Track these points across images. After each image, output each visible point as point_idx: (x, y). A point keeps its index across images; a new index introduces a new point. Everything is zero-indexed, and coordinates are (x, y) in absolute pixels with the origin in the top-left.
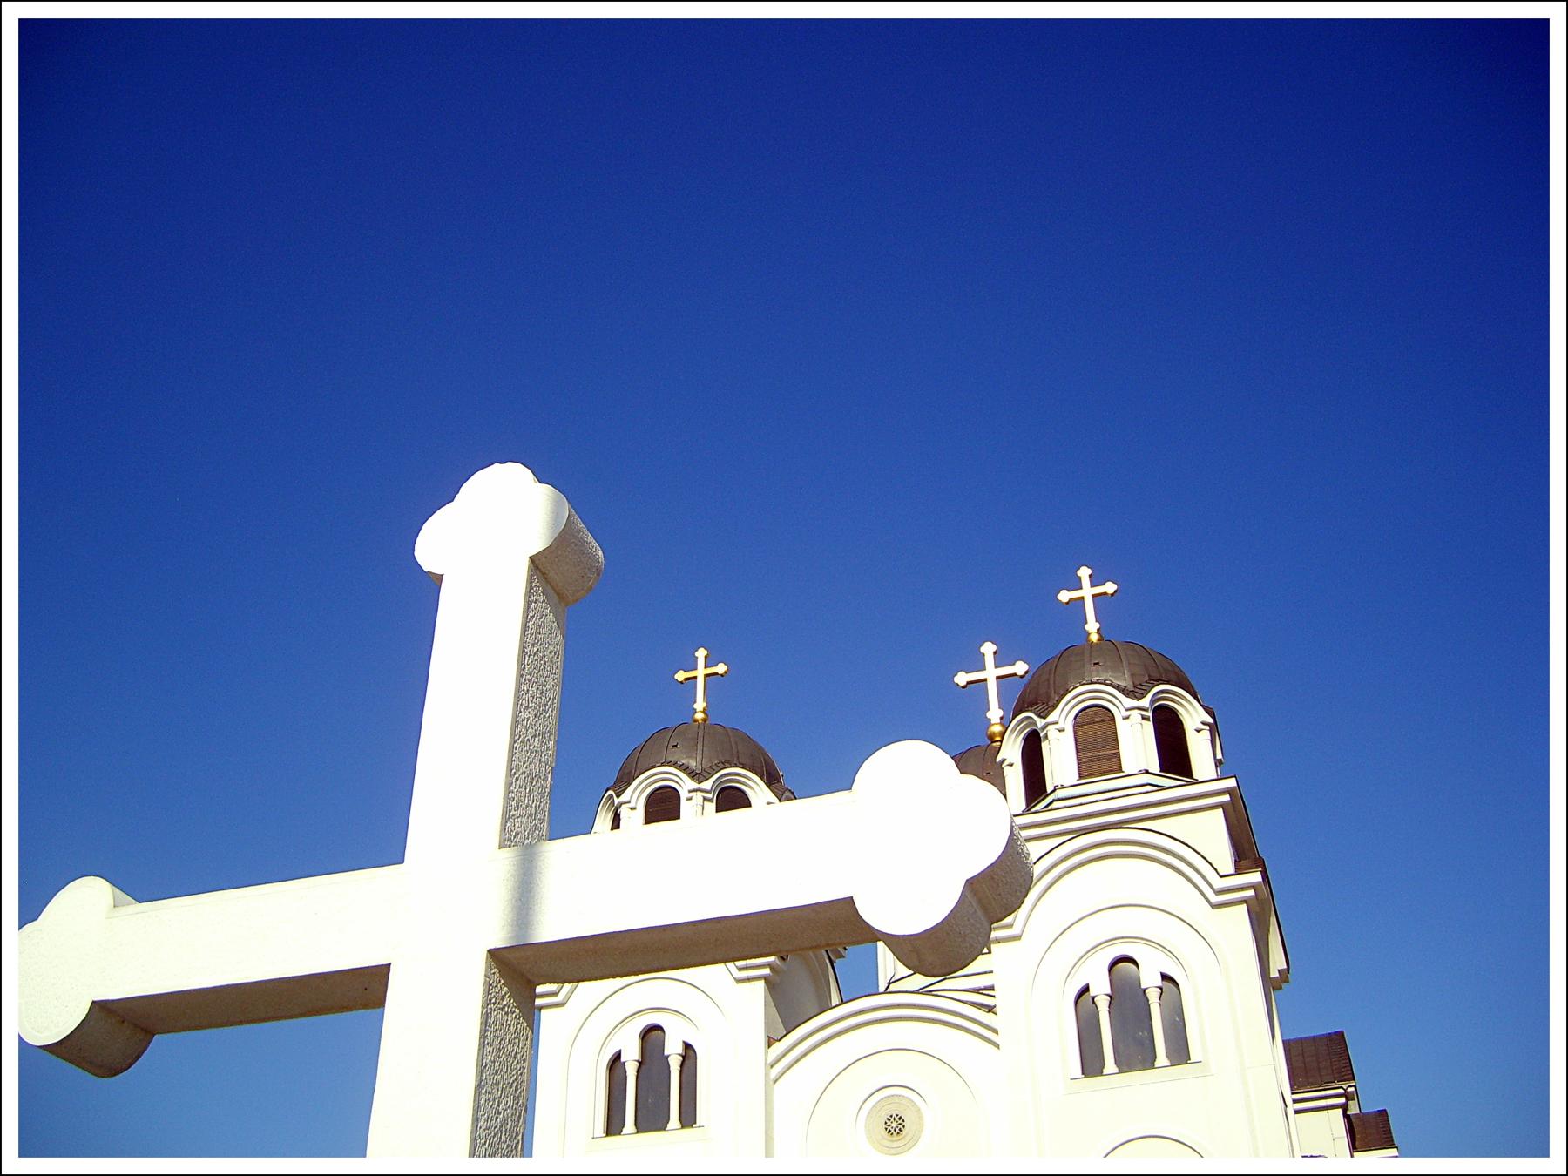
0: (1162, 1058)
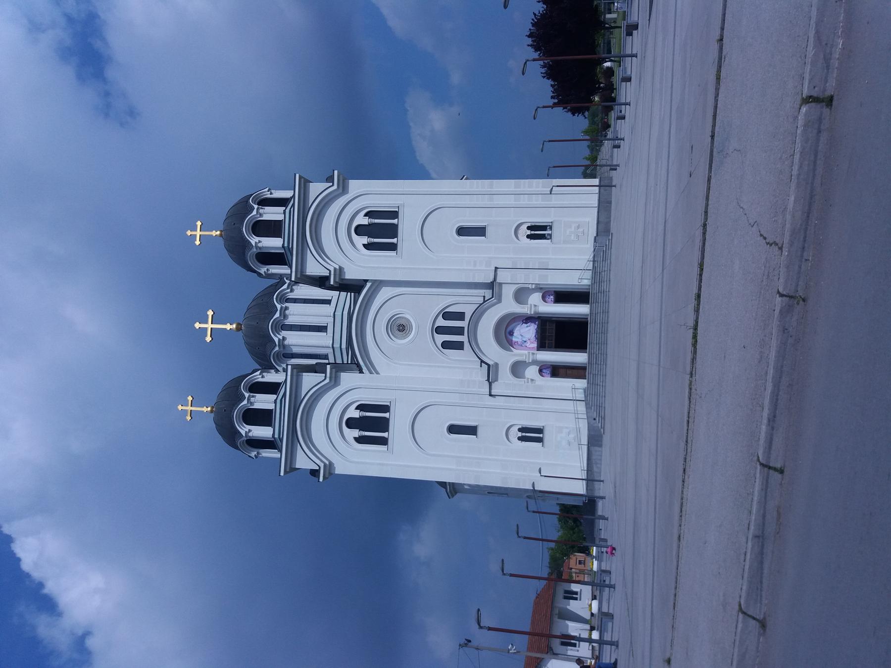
0: (395, 221)
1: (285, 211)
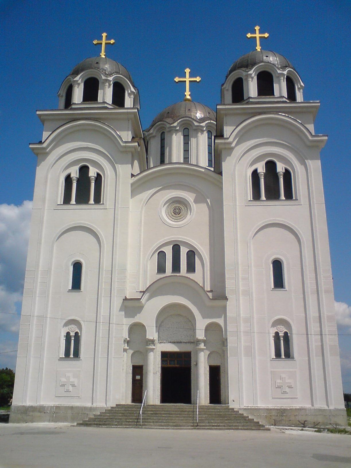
1: (284, 97)
